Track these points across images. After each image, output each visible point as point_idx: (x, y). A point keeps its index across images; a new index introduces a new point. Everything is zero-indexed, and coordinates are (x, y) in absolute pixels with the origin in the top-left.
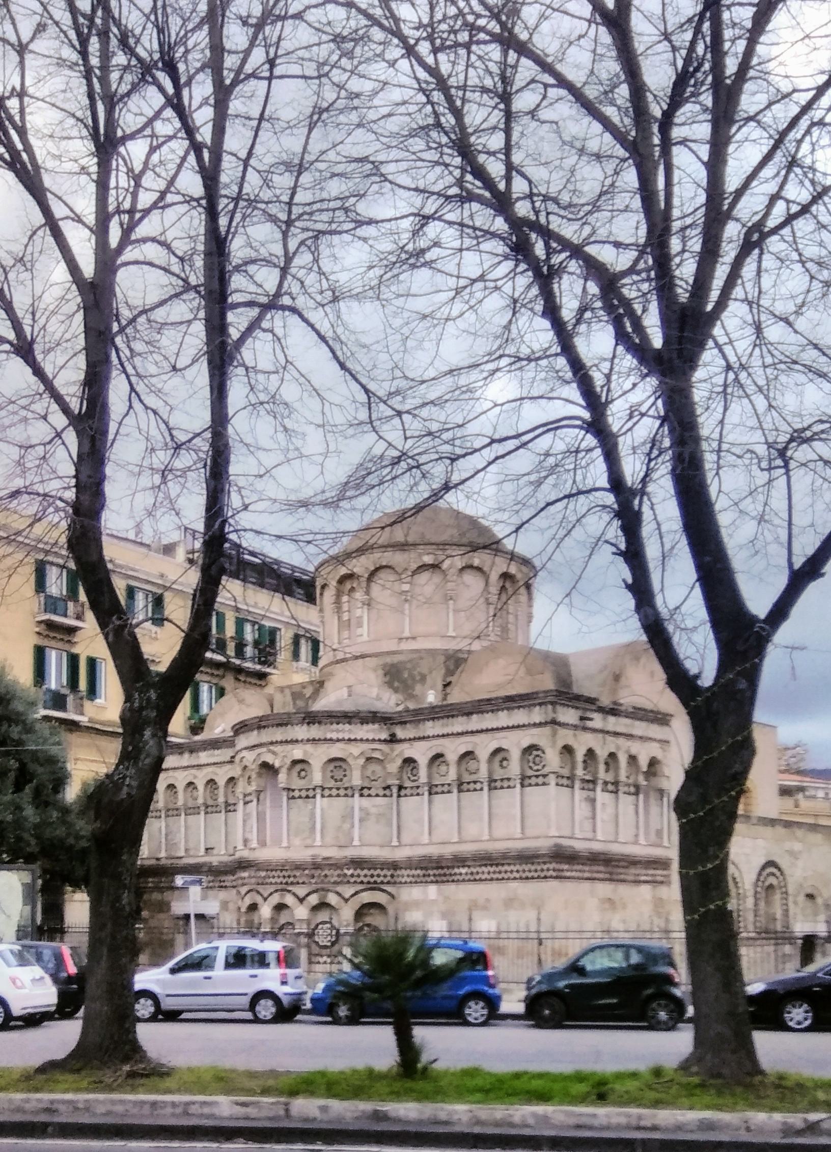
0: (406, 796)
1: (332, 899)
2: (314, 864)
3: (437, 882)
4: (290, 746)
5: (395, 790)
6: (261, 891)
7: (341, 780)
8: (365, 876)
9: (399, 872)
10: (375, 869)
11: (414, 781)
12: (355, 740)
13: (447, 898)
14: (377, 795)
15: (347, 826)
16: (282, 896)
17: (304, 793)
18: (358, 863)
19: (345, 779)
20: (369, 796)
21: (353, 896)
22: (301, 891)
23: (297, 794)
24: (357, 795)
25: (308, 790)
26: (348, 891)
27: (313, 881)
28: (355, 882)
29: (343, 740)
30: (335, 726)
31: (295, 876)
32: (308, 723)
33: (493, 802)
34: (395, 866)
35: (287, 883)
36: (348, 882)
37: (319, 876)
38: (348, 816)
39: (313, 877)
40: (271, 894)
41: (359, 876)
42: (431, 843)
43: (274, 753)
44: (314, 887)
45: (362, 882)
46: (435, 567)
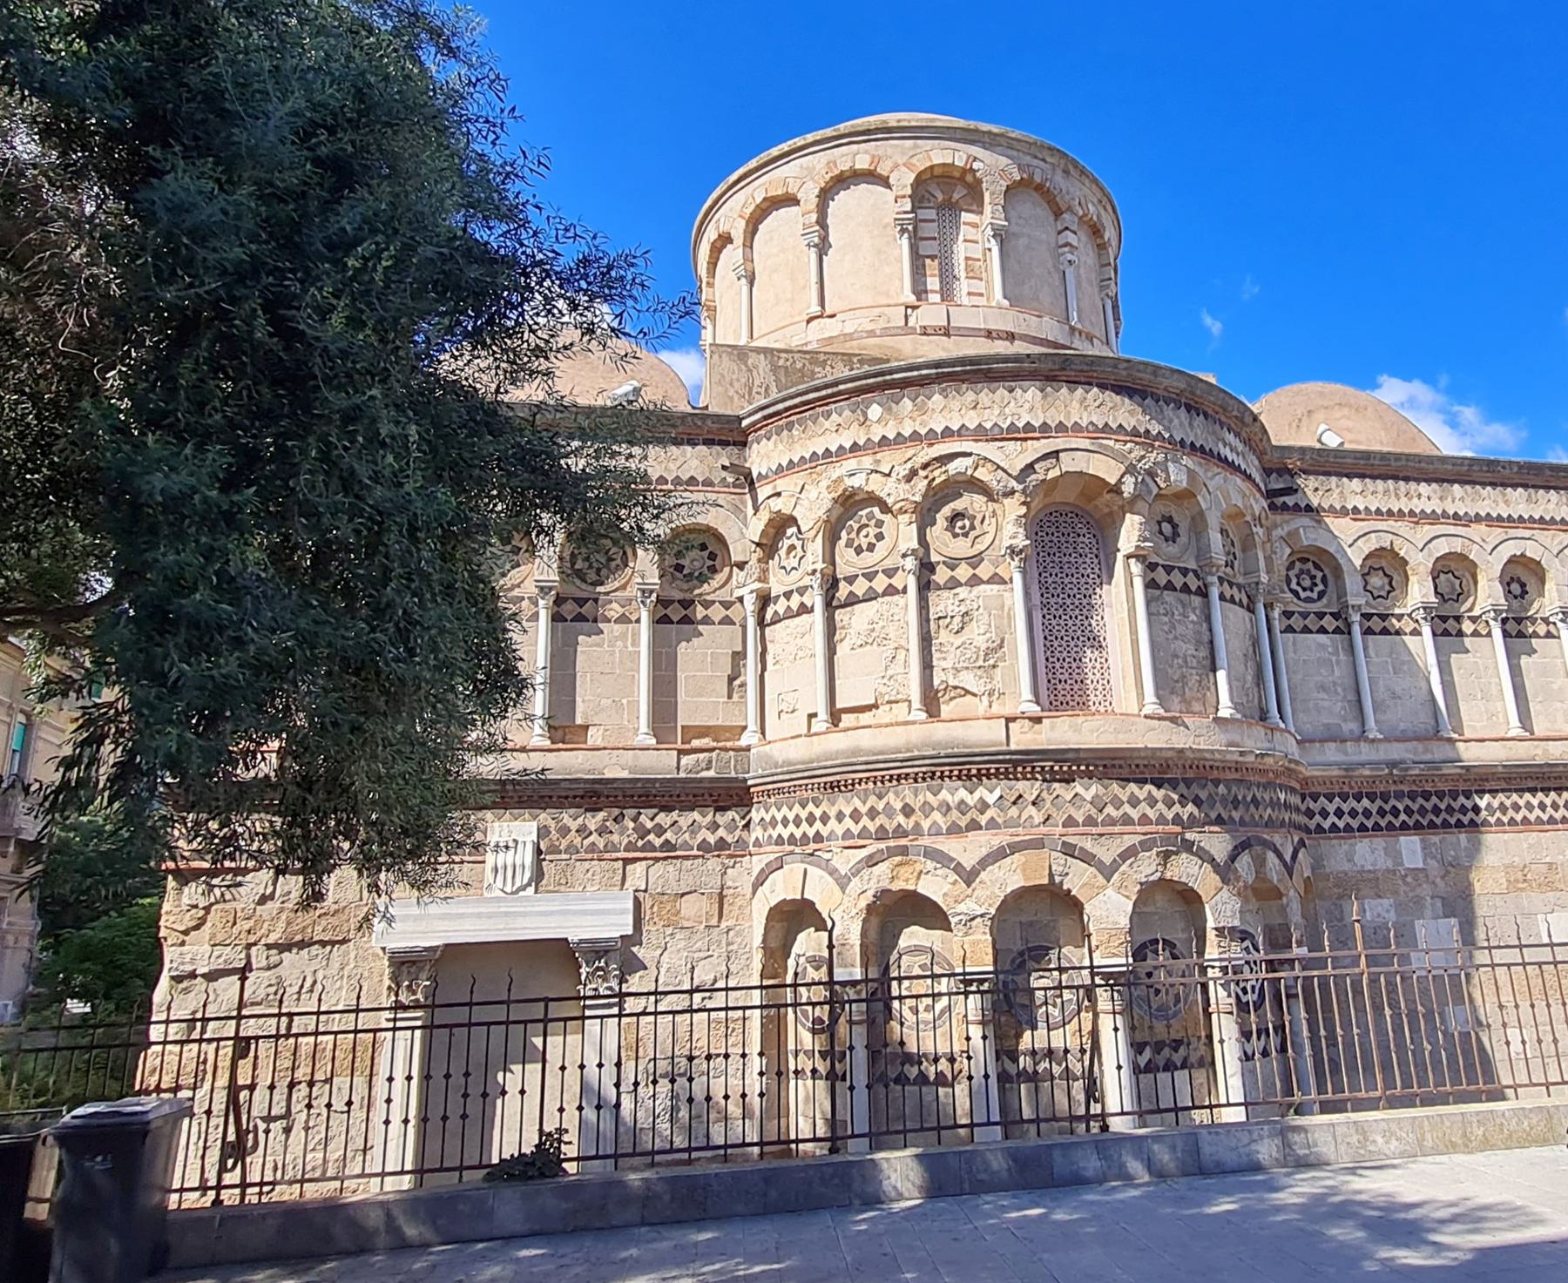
6: (1088, 844)
11: (1308, 600)
27: (1236, 815)
39: (1236, 803)
40: (1129, 854)
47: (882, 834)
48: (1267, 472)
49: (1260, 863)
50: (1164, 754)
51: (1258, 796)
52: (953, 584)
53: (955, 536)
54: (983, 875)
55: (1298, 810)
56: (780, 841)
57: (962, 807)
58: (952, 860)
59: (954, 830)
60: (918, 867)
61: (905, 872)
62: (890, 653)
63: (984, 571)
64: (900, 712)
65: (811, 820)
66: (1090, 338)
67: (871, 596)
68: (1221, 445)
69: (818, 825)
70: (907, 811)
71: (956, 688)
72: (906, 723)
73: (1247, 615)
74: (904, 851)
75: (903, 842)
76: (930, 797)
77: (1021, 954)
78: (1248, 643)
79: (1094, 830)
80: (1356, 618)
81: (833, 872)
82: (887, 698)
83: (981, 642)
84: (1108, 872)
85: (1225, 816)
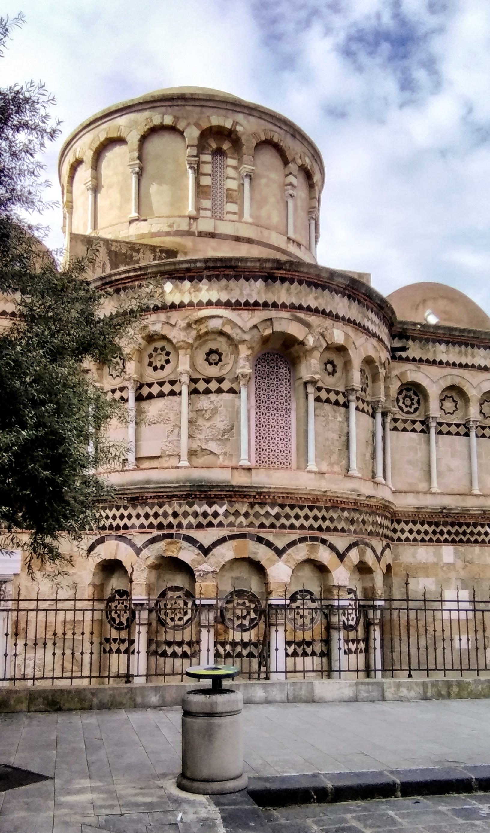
3: (453, 541)
4: (329, 322)
13: (468, 563)
16: (312, 549)
18: (385, 508)
22: (341, 543)
25: (337, 393)
27: (352, 528)
31: (332, 520)
32: (349, 297)
34: (395, 517)
35: (320, 529)
36: (378, 534)
39: (352, 522)
40: (293, 544)
43: (307, 325)
44: (353, 538)
47: (160, 526)
48: (393, 336)
49: (362, 553)
50: (315, 493)
51: (366, 519)
52: (207, 391)
53: (210, 364)
54: (214, 551)
55: (387, 528)
56: (104, 528)
57: (205, 515)
58: (198, 542)
59: (200, 526)
60: (179, 545)
61: (173, 547)
62: (169, 427)
63: (225, 386)
64: (173, 462)
65: (122, 517)
66: (299, 245)
67: (161, 395)
68: (366, 320)
69: (126, 520)
70: (175, 515)
71: (206, 449)
72: (177, 468)
73: (371, 419)
74: (170, 536)
75: (171, 531)
76: (187, 508)
77: (231, 593)
78: (370, 435)
79: (274, 531)
80: (433, 424)
81: (133, 545)
82: (167, 453)
83: (221, 426)
84: (280, 553)
85: (346, 528)
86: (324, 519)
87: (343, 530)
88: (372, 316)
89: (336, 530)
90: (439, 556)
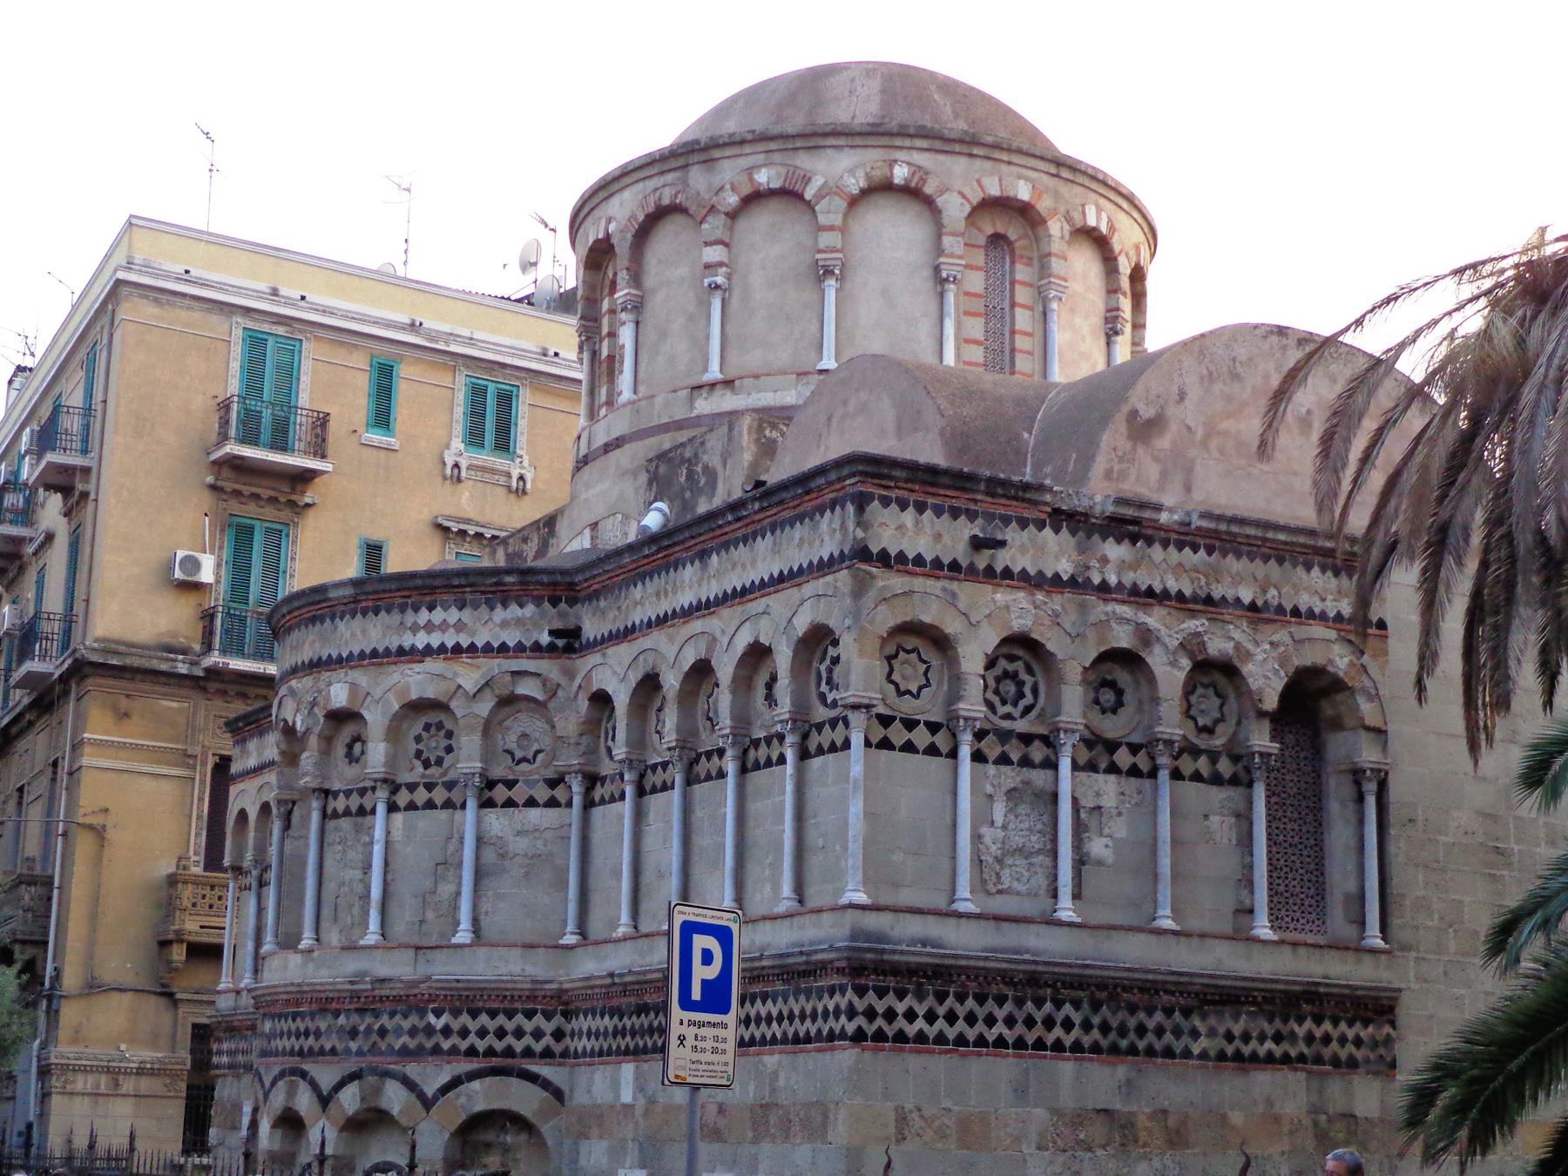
0: (603, 801)
1: (394, 1098)
2: (355, 996)
5: (577, 787)
7: (439, 762)
8: (482, 1033)
9: (575, 1024)
10: (510, 1015)
12: (472, 648)
14: (531, 803)
15: (446, 889)
17: (354, 802)
19: (448, 760)
20: (510, 803)
21: (445, 1089)
23: (340, 804)
24: (471, 804)
26: (433, 1077)
27: (354, 1046)
28: (454, 1051)
29: (442, 648)
30: (424, 616)
31: (318, 1034)
33: (753, 807)
34: (564, 1004)
35: (301, 1053)
36: (436, 1050)
37: (369, 1029)
38: (446, 865)
39: (353, 1033)
41: (464, 1033)
42: (637, 935)
44: (351, 1066)
45: (472, 1052)
46: (789, 194)
85: (340, 1047)
86: (307, 1034)
87: (333, 1051)
88: (438, 615)
89: (322, 1052)
90: (615, 1086)
